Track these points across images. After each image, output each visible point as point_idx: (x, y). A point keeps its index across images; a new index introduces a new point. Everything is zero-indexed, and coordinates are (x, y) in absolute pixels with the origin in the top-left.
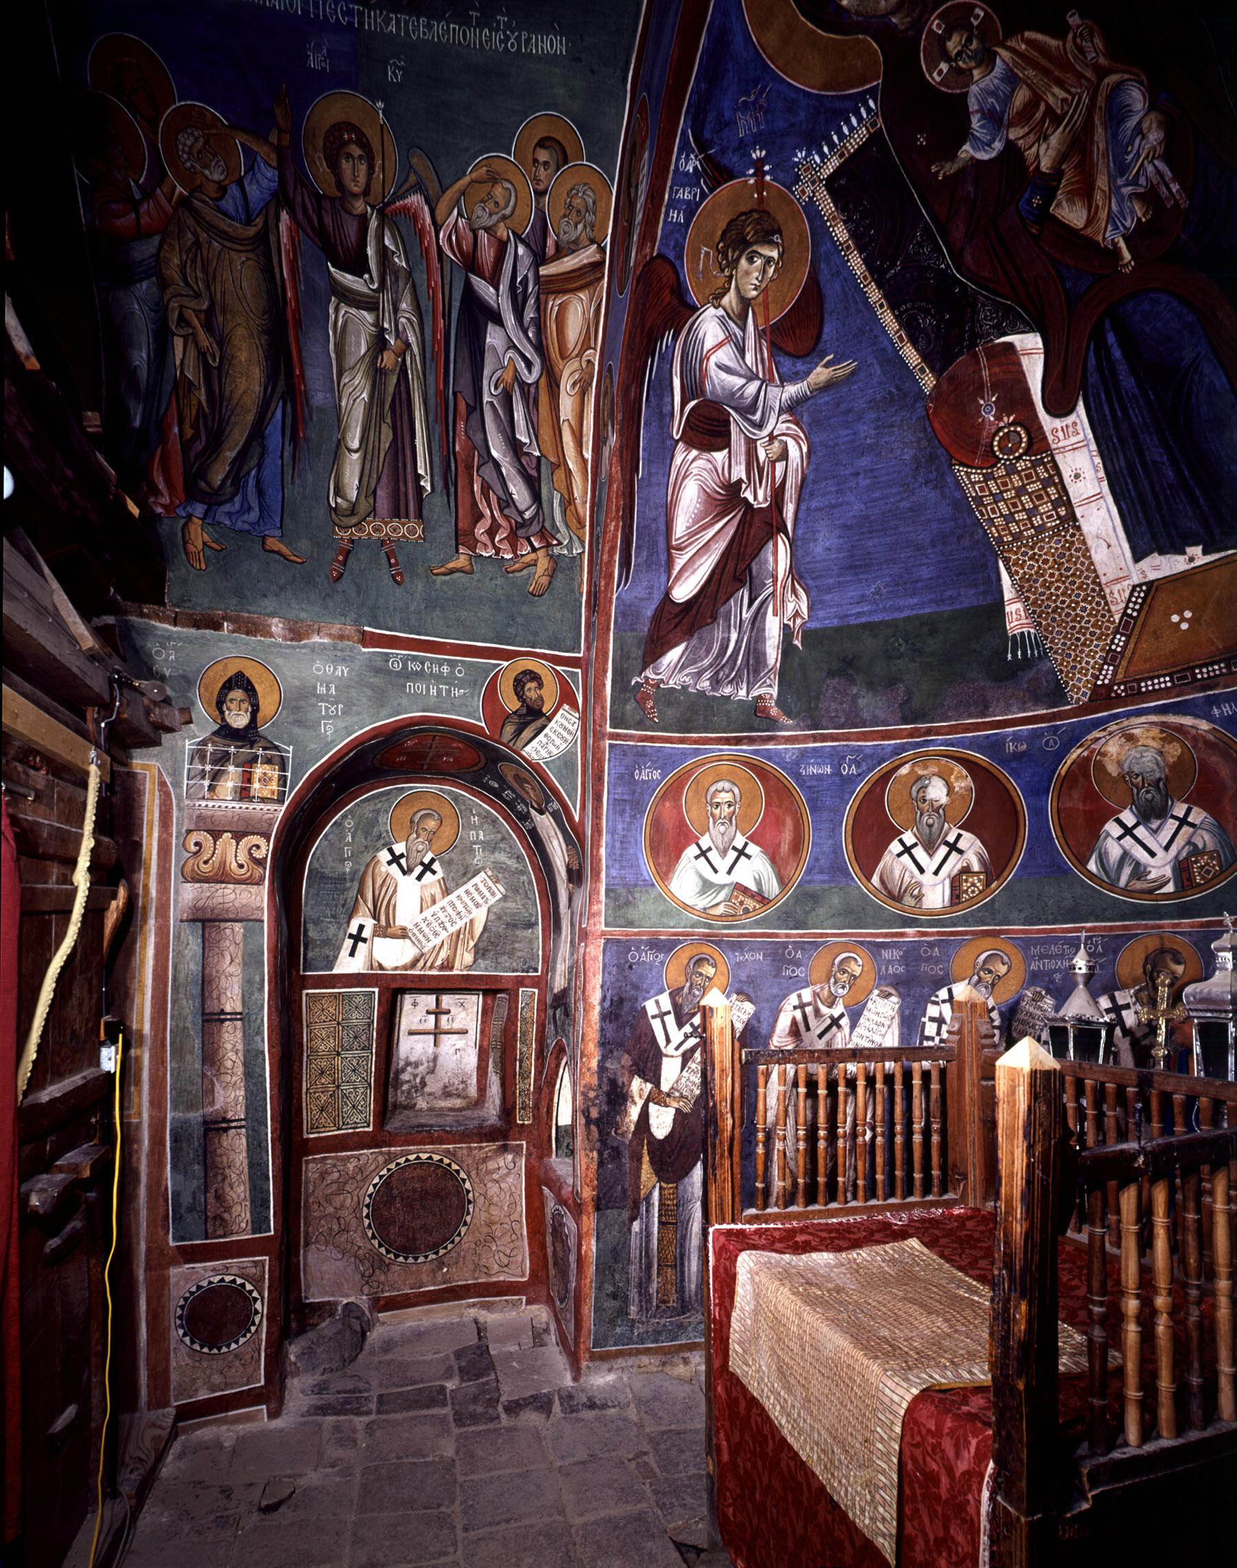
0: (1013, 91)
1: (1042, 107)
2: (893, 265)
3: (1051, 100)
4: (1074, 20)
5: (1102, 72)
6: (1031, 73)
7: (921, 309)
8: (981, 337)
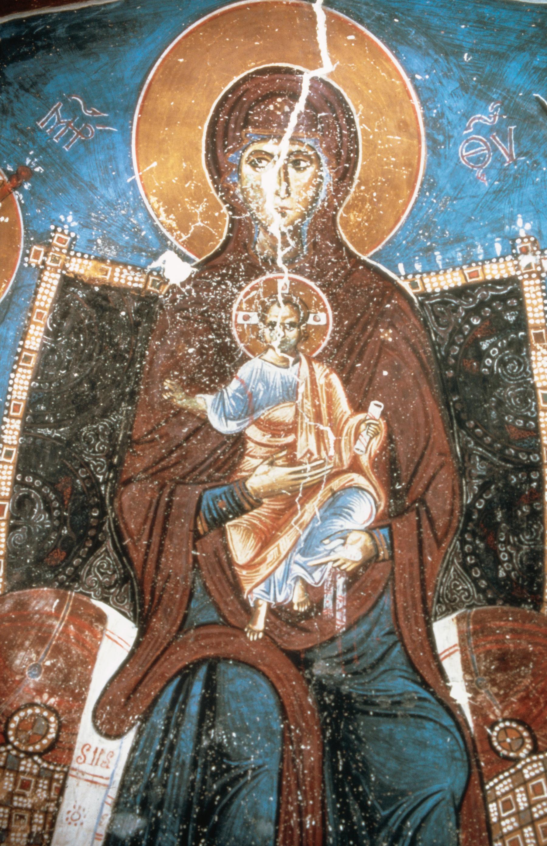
1: (290, 439)
2: (57, 425)
4: (375, 409)
5: (355, 466)
6: (308, 405)
7: (46, 500)
8: (82, 584)
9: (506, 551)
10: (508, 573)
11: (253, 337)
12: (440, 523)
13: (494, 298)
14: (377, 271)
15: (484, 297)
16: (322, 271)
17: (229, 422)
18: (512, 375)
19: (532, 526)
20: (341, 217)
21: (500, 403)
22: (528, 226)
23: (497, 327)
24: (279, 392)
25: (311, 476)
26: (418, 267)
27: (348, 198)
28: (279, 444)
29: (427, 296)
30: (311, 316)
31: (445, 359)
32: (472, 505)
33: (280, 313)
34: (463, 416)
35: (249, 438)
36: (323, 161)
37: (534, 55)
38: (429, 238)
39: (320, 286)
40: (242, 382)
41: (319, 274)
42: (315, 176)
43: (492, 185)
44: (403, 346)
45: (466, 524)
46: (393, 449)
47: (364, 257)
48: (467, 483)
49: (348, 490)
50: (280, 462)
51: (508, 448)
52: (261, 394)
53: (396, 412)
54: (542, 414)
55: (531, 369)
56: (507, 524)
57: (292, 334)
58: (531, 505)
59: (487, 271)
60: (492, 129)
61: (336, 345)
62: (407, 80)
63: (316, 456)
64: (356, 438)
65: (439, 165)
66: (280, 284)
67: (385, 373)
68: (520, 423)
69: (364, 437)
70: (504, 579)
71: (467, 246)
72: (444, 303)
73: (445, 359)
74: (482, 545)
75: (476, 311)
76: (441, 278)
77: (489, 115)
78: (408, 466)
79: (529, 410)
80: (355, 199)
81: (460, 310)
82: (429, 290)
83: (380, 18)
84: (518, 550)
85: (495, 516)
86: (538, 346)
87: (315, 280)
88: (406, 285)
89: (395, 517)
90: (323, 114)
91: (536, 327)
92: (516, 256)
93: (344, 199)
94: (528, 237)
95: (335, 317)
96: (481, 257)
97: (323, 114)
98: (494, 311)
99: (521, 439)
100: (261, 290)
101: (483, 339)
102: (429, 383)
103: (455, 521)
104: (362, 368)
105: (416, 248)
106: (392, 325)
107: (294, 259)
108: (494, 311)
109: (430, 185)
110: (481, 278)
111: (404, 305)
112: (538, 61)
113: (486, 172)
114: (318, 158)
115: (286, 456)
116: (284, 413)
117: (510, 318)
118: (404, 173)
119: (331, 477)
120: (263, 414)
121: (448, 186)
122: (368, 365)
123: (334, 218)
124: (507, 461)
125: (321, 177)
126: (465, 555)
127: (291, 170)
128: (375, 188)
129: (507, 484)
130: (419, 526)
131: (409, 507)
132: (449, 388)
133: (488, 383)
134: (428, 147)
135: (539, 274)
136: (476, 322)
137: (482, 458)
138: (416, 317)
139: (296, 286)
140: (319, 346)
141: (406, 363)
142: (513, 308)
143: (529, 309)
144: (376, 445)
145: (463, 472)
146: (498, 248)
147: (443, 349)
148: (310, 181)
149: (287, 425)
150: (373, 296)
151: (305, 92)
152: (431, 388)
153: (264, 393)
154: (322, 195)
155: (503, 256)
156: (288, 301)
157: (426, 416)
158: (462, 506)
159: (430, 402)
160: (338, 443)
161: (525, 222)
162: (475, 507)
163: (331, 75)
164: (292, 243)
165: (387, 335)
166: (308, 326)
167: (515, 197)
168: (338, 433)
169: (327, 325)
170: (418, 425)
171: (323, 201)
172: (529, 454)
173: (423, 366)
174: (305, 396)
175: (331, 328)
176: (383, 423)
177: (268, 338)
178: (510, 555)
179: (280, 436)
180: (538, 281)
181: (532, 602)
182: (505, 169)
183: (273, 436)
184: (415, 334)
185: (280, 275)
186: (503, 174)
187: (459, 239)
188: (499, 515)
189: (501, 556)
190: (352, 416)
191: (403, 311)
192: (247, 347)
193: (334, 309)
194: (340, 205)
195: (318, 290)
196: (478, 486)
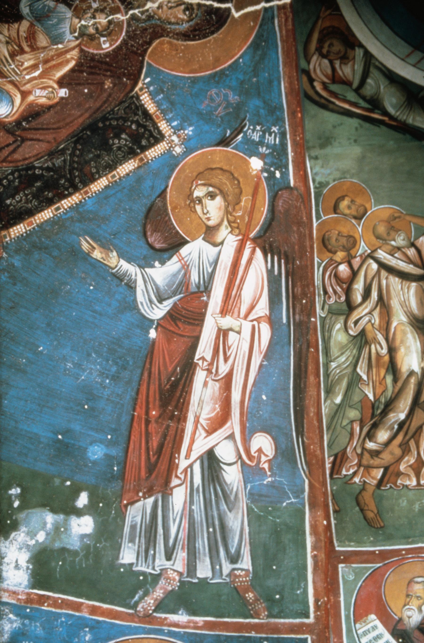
0: (50, 38)
1: (27, 49)
3: (27, 56)
4: (63, 92)
5: (25, 94)
6: (52, 53)
9: (21, 198)
10: (11, 204)
11: (84, 7)
12: (16, 156)
13: (150, 131)
14: (141, 68)
15: (149, 126)
16: (133, 37)
17: (28, 8)
18: (116, 156)
19: (43, 202)
20: (164, 40)
21: (98, 156)
22: (191, 133)
23: (136, 138)
24: (55, 33)
25: (8, 70)
26: (152, 88)
27: (175, 41)
28: (22, 44)
29: (138, 97)
30: (105, 39)
31: (107, 119)
32: (34, 168)
33: (103, 20)
34: (81, 141)
35: (20, 23)
36: (191, 23)
37: (264, 108)
38: (168, 89)
39: (124, 39)
40: (55, 8)
41: (131, 36)
42: (183, 20)
43: (203, 110)
44: (105, 95)
45: (23, 170)
46: (44, 112)
47: (146, 58)
48: (46, 159)
49: (8, 96)
50: (10, 48)
51: (77, 170)
52: (51, 22)
53: (67, 104)
54: (105, 178)
55: (124, 163)
56: (37, 190)
57: (92, 31)
58: (54, 196)
59: (162, 123)
60: (228, 101)
61: (93, 57)
62: (238, 56)
63: (21, 68)
64: (42, 88)
65: (204, 82)
66: (119, 16)
67: (86, 91)
68: (94, 170)
69: (45, 93)
70: (6, 204)
71: (171, 109)
72: (137, 108)
73: (107, 119)
74: (17, 184)
75: (139, 125)
76: (150, 102)
77: (234, 98)
78: (39, 124)
79: (103, 171)
80: (176, 45)
81: (137, 117)
82: (141, 98)
83: (263, 36)
84: (27, 202)
85: (36, 182)
86: (137, 161)
87: (126, 35)
88: (140, 85)
89: (6, 130)
90: (214, 18)
91: (146, 156)
92: (175, 133)
93: (174, 39)
94: (186, 135)
95: (109, 52)
96: (167, 117)
97: (214, 18)
98: (143, 134)
99: (85, 175)
100: (113, 5)
101: (127, 134)
102: (91, 116)
103: (21, 163)
104: (85, 77)
105: (161, 84)
106: (115, 85)
107: (135, 20)
108: (143, 134)
109: (194, 81)
110: (157, 121)
111: (129, 88)
112: (262, 111)
113: (208, 105)
114: (192, 20)
115: (15, 50)
116: (42, 40)
117: (144, 142)
118: (196, 66)
119: (12, 83)
120: (38, 27)
121: (196, 90)
122: (87, 80)
123: (162, 36)
124: (70, 173)
125: (182, 24)
126: (6, 178)
127: (183, 7)
128: (184, 54)
129: (58, 180)
130: (8, 145)
131: (15, 135)
132: (92, 127)
133: (106, 147)
134: (210, 74)
135: (171, 146)
136: (134, 127)
137: (65, 161)
138: (124, 96)
139: (119, 24)
140: (89, 48)
141: (96, 100)
142: (149, 142)
143: (153, 149)
144: (43, 101)
145: (51, 154)
146: (175, 123)
147: (112, 116)
148: (180, 18)
149: (35, 44)
150: (127, 70)
151: (223, 6)
152: (88, 118)
153: (52, 24)
154: (173, 27)
155: (172, 127)
156: (110, 22)
157: (72, 122)
158: (32, 163)
159: (80, 120)
160: (35, 78)
161: (192, 131)
162: (35, 170)
163: (233, 17)
164: (144, 17)
165: (108, 84)
166: (99, 38)
167: (201, 122)
168: (41, 76)
169: (103, 49)
170: (64, 119)
171: (170, 28)
172: (80, 182)
173: (98, 109)
174: (57, 49)
175: (102, 52)
176: (56, 100)
177: (86, 16)
178: (21, 200)
179: (27, 42)
180: (167, 148)
181: (3, 225)
182: (213, 114)
183: (26, 38)
184: (114, 99)
185: (124, 14)
186: (210, 113)
187: (172, 103)
188: (38, 184)
189: (17, 196)
190: (54, 81)
191: (125, 88)
192: (77, 6)
193: (113, 50)
194: (170, 38)
195: (121, 38)
196: (48, 166)
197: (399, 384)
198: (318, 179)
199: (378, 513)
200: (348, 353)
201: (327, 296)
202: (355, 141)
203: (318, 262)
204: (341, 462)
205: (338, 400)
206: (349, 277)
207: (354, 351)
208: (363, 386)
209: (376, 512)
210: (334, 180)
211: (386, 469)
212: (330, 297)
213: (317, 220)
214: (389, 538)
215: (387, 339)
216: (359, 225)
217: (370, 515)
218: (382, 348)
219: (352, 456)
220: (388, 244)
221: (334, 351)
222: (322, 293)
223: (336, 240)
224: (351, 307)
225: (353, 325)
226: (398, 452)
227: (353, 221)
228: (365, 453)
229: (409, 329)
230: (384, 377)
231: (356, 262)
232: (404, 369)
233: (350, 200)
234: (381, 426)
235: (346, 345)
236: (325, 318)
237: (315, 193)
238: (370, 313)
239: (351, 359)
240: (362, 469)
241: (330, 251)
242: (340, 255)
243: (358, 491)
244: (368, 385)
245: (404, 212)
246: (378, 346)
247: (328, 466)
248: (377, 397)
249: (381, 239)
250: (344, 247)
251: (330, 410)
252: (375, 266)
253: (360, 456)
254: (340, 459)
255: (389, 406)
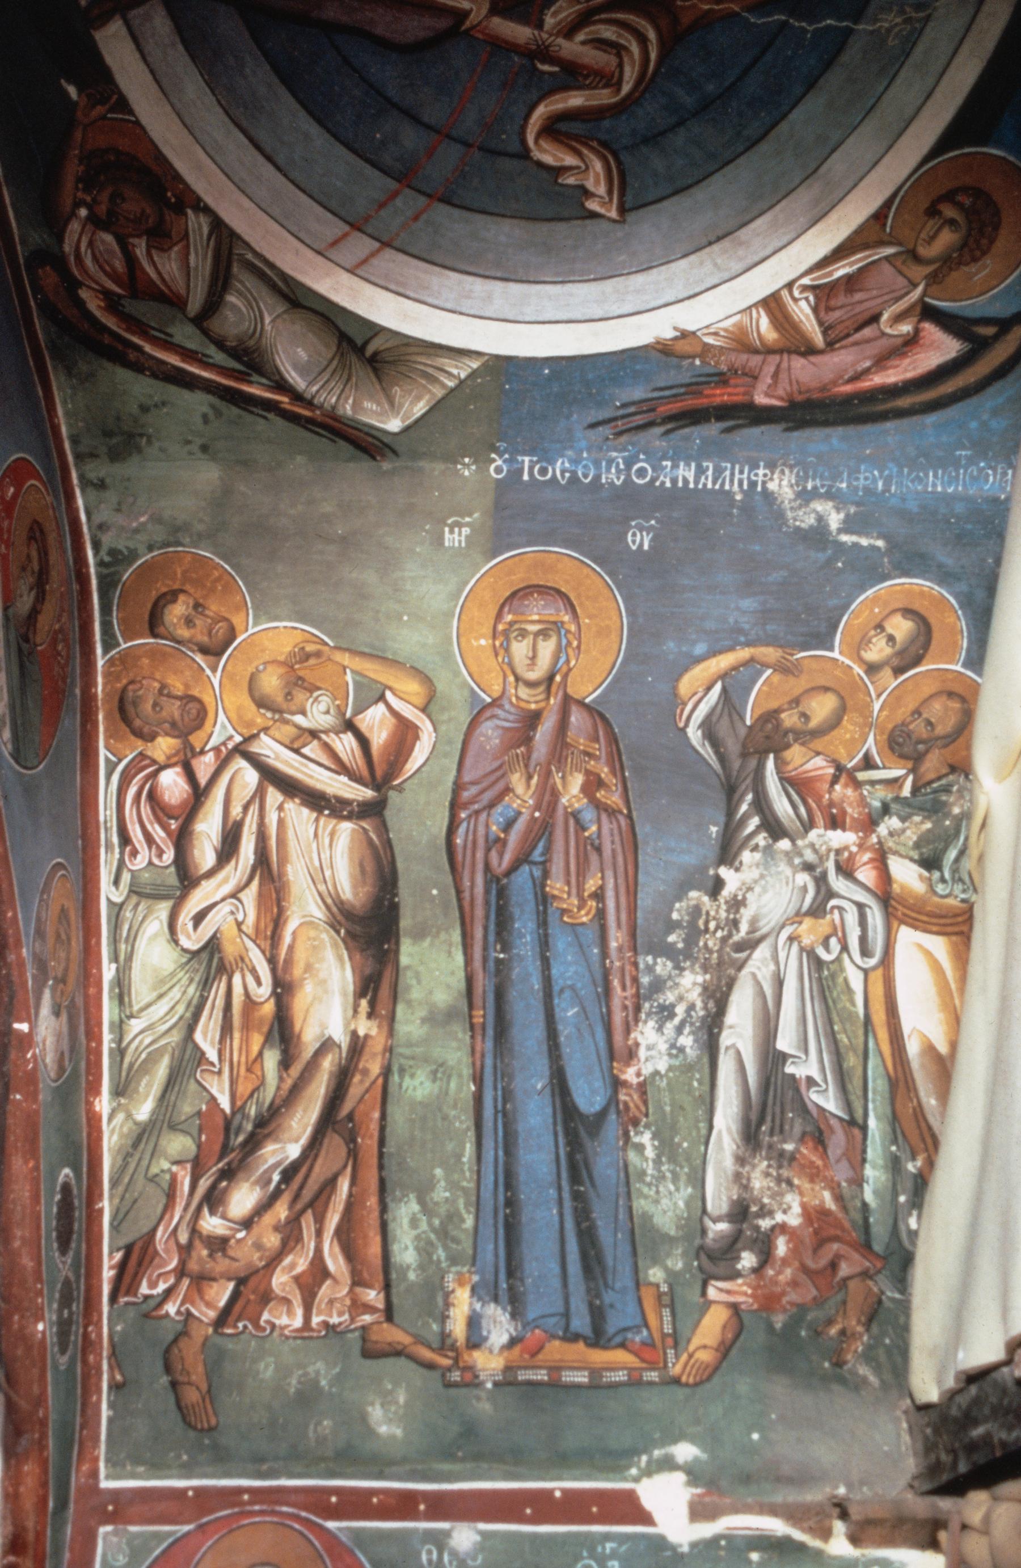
197: (295, 1071)
198: (108, 540)
199: (209, 1391)
200: (176, 994)
201: (128, 849)
202: (204, 448)
203: (107, 760)
204: (140, 1264)
205: (144, 1111)
206: (184, 803)
207: (191, 990)
208: (206, 1075)
209: (204, 1387)
210: (150, 548)
211: (241, 1282)
212: (134, 853)
213: (106, 650)
214: (222, 1459)
215: (272, 961)
216: (214, 670)
217: (192, 1396)
218: (259, 983)
219: (167, 1251)
220: (287, 722)
221: (141, 991)
222: (115, 840)
223: (155, 705)
224: (187, 878)
225: (190, 925)
226: (273, 1241)
227: (199, 658)
228: (197, 1243)
229: (326, 937)
230: (260, 1054)
231: (204, 766)
232: (310, 1036)
233: (191, 602)
234: (241, 1175)
235: (173, 974)
236: (122, 904)
237: (101, 578)
238: (234, 895)
239: (180, 1009)
240: (186, 1282)
241: (139, 734)
242: (164, 746)
243: (171, 1337)
244: (220, 1073)
245: (331, 644)
246: (250, 980)
247: (108, 1274)
248: (239, 1103)
249: (268, 708)
250: (174, 724)
251: (122, 1136)
252: (251, 777)
253: (186, 1251)
254: (137, 1258)
255: (267, 1124)
